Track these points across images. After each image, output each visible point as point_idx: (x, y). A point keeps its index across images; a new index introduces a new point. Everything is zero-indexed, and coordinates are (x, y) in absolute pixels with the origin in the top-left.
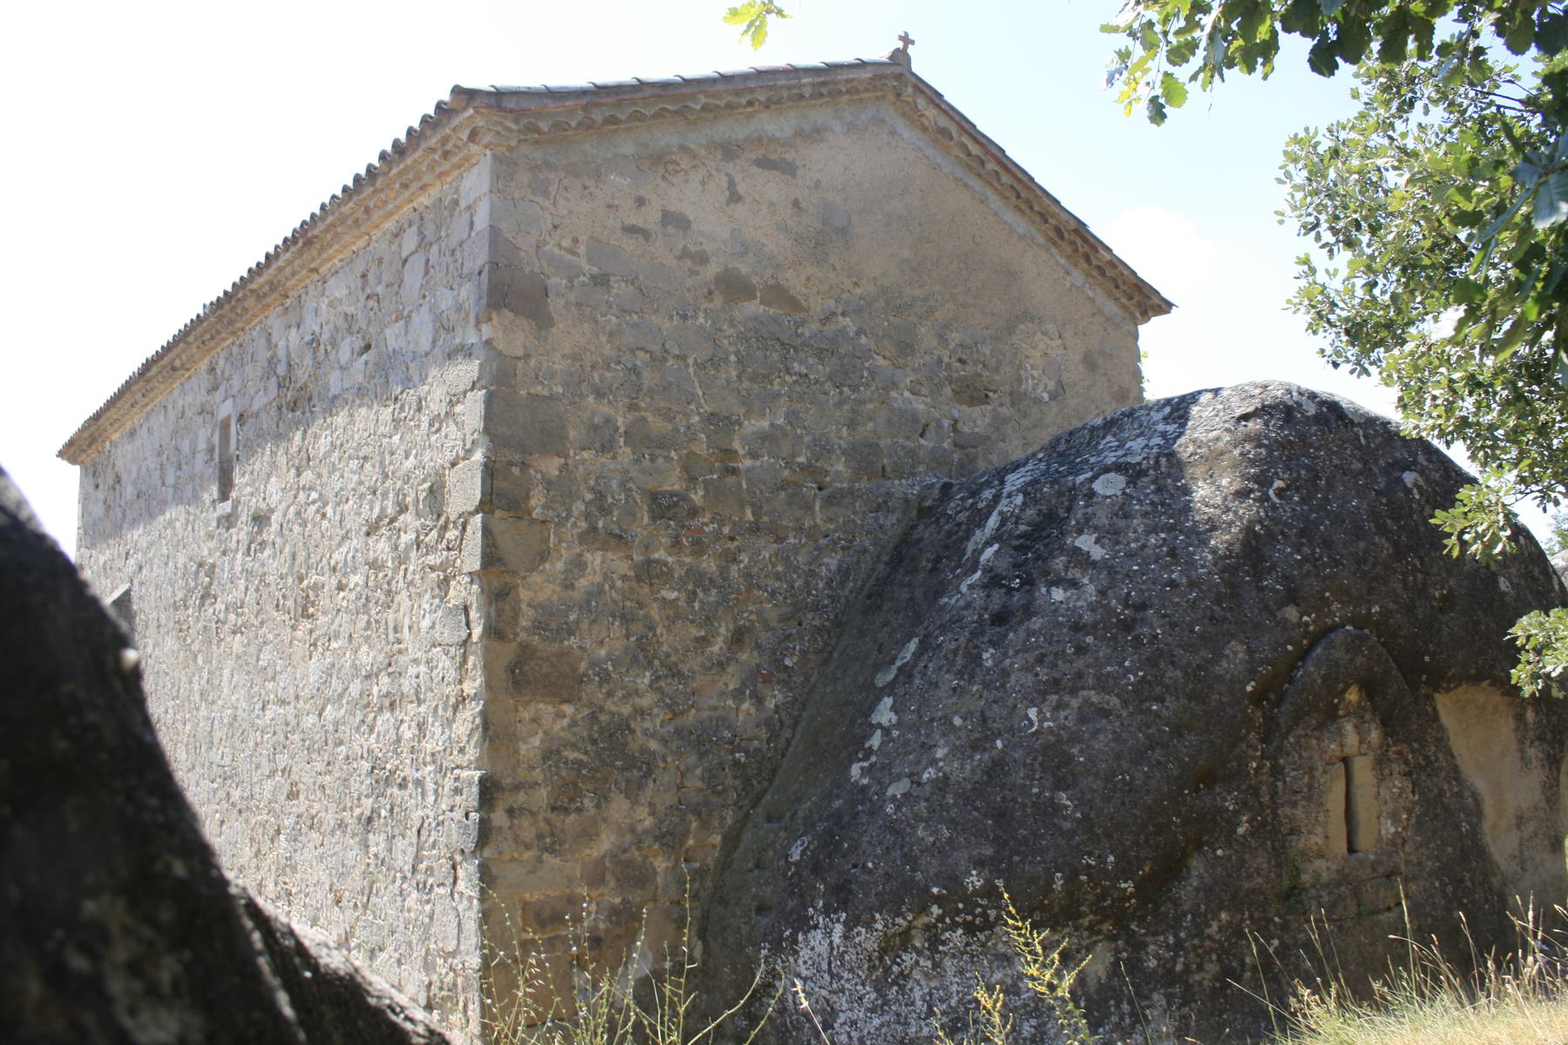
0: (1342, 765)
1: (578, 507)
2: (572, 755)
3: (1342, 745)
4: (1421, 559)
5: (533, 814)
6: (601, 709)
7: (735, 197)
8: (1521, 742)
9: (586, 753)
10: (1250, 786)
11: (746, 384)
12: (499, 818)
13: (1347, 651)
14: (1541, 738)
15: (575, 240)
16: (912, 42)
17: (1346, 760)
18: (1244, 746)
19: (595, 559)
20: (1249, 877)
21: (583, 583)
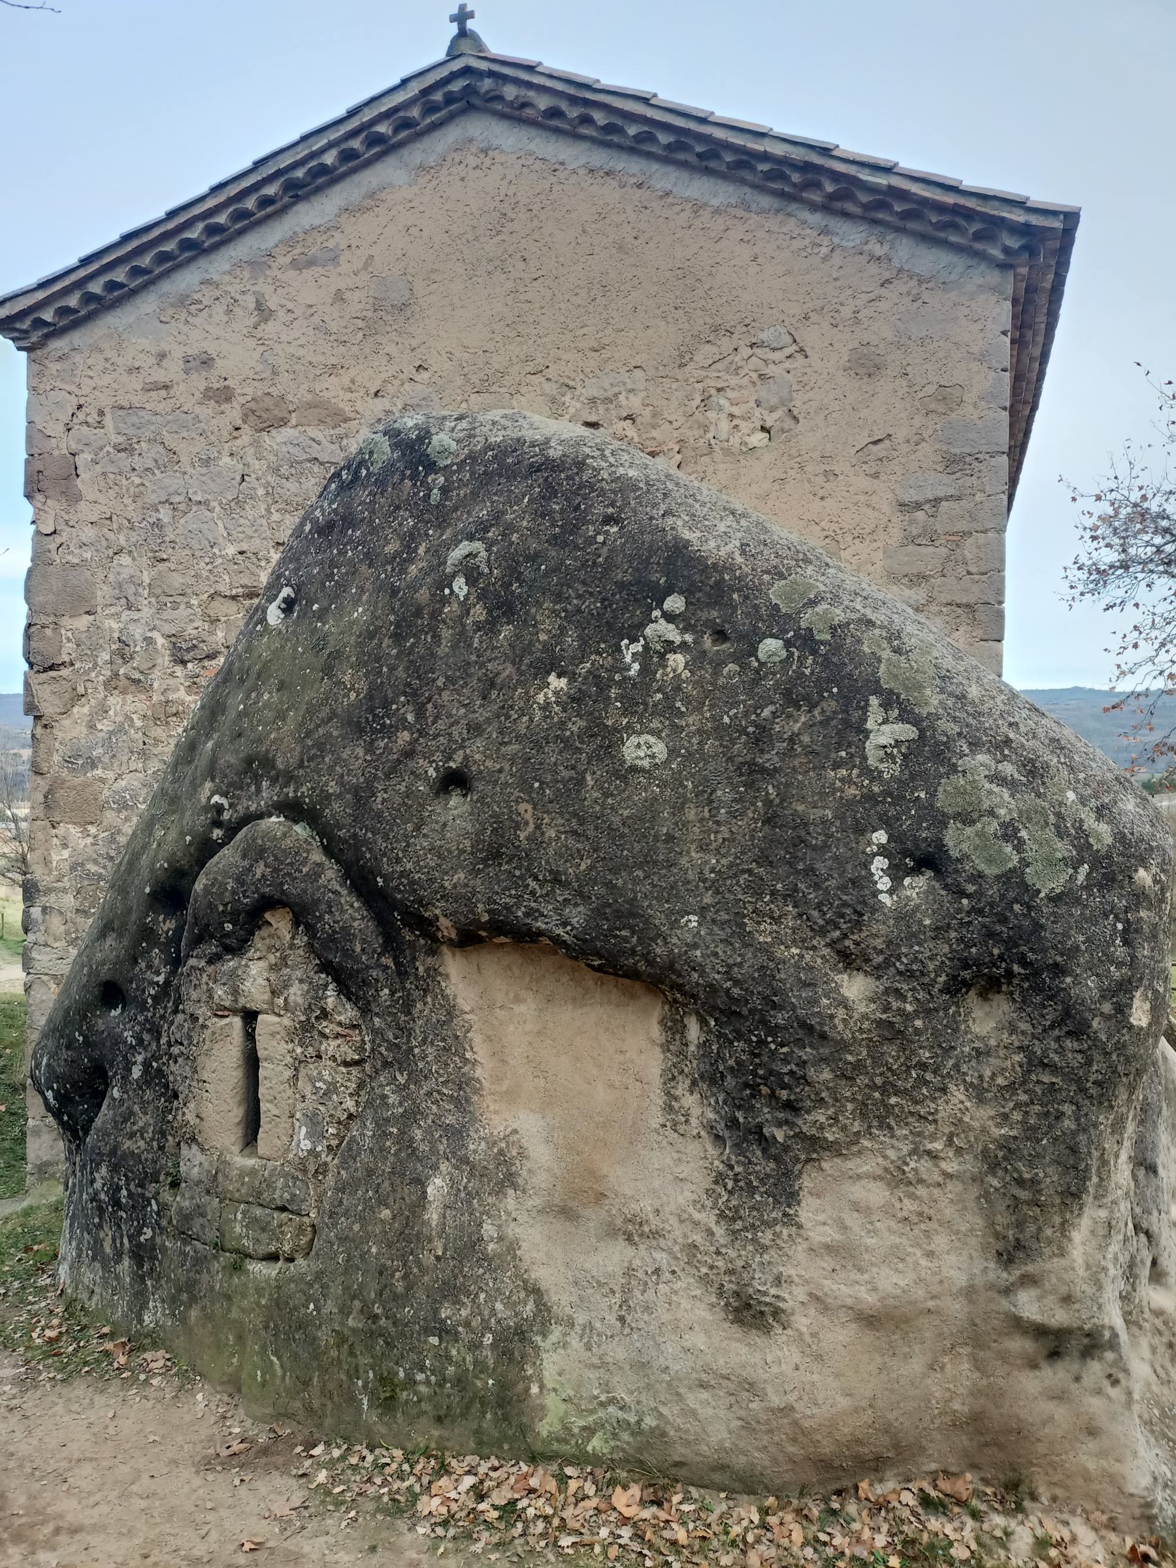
0: (237, 1022)
1: (105, 656)
2: (93, 868)
3: (235, 992)
4: (420, 713)
5: (61, 913)
6: (119, 832)
7: (263, 312)
8: (670, 1078)
9: (104, 867)
10: (146, 1020)
11: (276, 516)
12: (36, 912)
13: (244, 857)
14: (713, 1079)
15: (101, 413)
16: (471, 15)
17: (250, 1017)
18: (143, 965)
19: (114, 701)
20: (132, 1136)
21: (104, 726)
